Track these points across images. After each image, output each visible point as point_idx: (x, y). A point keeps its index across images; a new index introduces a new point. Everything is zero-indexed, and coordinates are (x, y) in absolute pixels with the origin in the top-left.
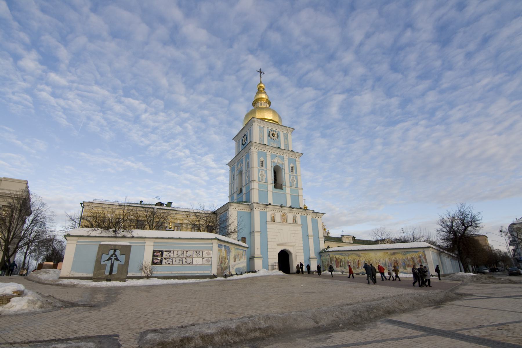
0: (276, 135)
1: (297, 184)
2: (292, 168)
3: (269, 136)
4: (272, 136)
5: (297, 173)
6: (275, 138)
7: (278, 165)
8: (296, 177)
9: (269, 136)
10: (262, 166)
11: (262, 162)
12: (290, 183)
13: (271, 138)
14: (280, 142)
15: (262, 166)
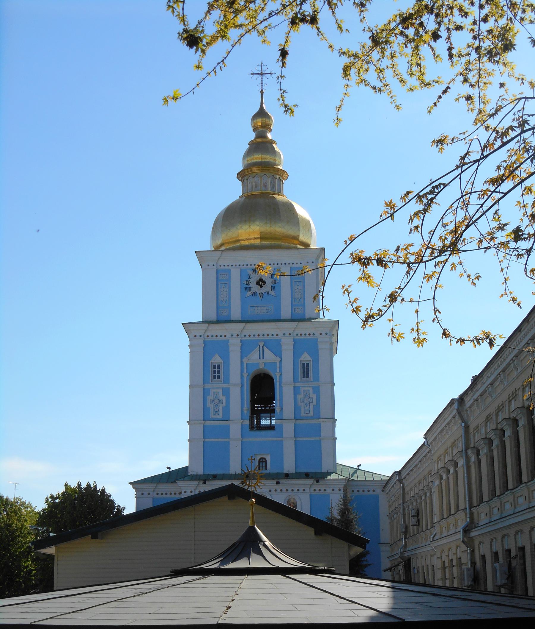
0: (269, 282)
1: (317, 408)
2: (306, 366)
3: (248, 289)
4: (255, 288)
5: (317, 378)
6: (267, 288)
7: (262, 366)
8: (316, 390)
9: (248, 289)
10: (216, 376)
11: (217, 367)
12: (296, 408)
13: (255, 294)
14: (278, 297)
15: (216, 376)
